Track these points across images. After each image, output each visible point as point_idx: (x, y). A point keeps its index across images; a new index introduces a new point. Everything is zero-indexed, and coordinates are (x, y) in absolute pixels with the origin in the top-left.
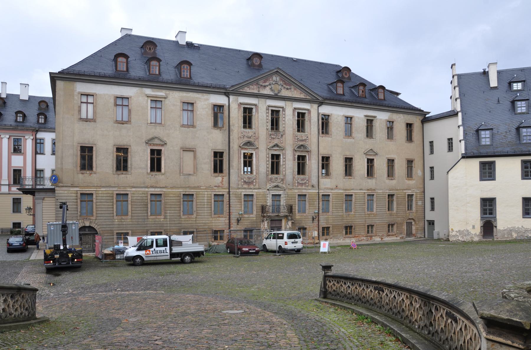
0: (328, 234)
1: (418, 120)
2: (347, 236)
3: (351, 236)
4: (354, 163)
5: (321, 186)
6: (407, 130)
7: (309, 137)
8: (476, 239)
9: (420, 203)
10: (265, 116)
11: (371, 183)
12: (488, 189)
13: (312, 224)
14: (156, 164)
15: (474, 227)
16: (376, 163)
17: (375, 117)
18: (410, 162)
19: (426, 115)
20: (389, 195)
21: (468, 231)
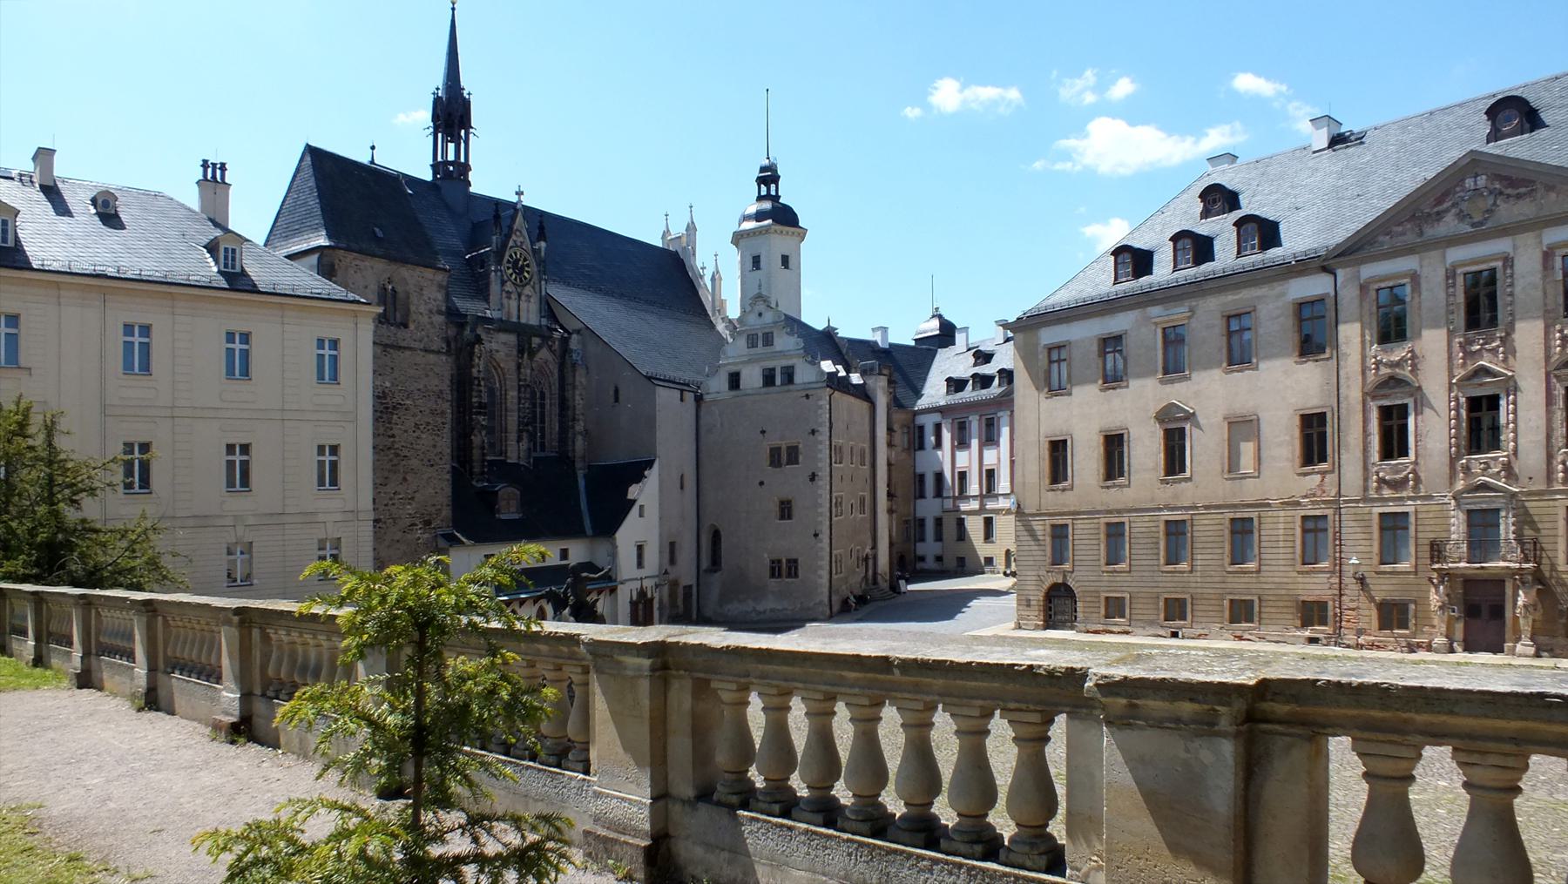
10: (1442, 295)
14: (1175, 460)
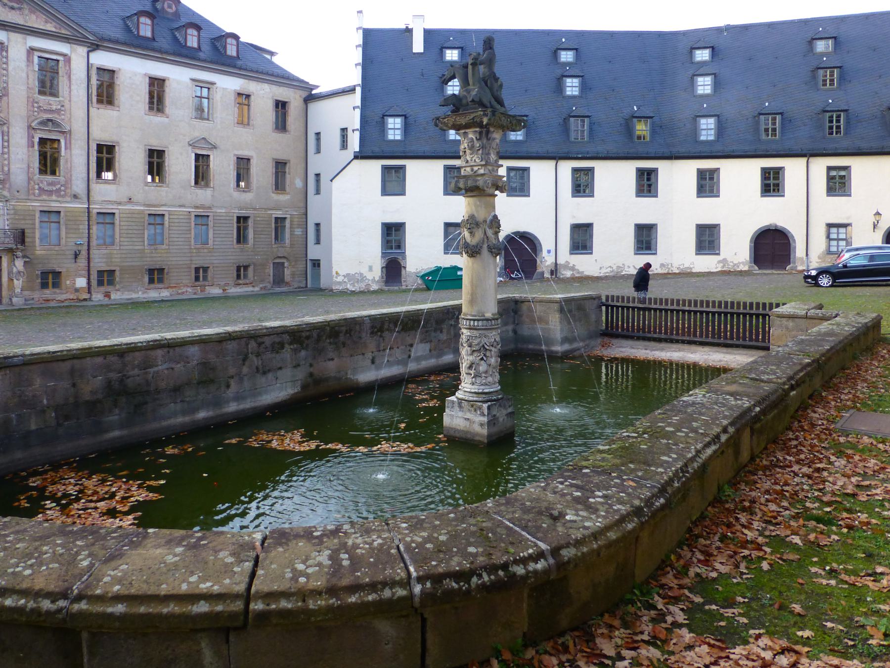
0: (111, 282)
1: (297, 97)
2: (152, 286)
3: (161, 286)
4: (167, 160)
5: (95, 196)
6: (277, 112)
7: (67, 106)
9: (298, 232)
11: (203, 196)
12: (394, 209)
13: (73, 265)
16: (213, 162)
17: (213, 84)
18: (280, 166)
19: (312, 89)
20: (239, 218)
21: (361, 274)
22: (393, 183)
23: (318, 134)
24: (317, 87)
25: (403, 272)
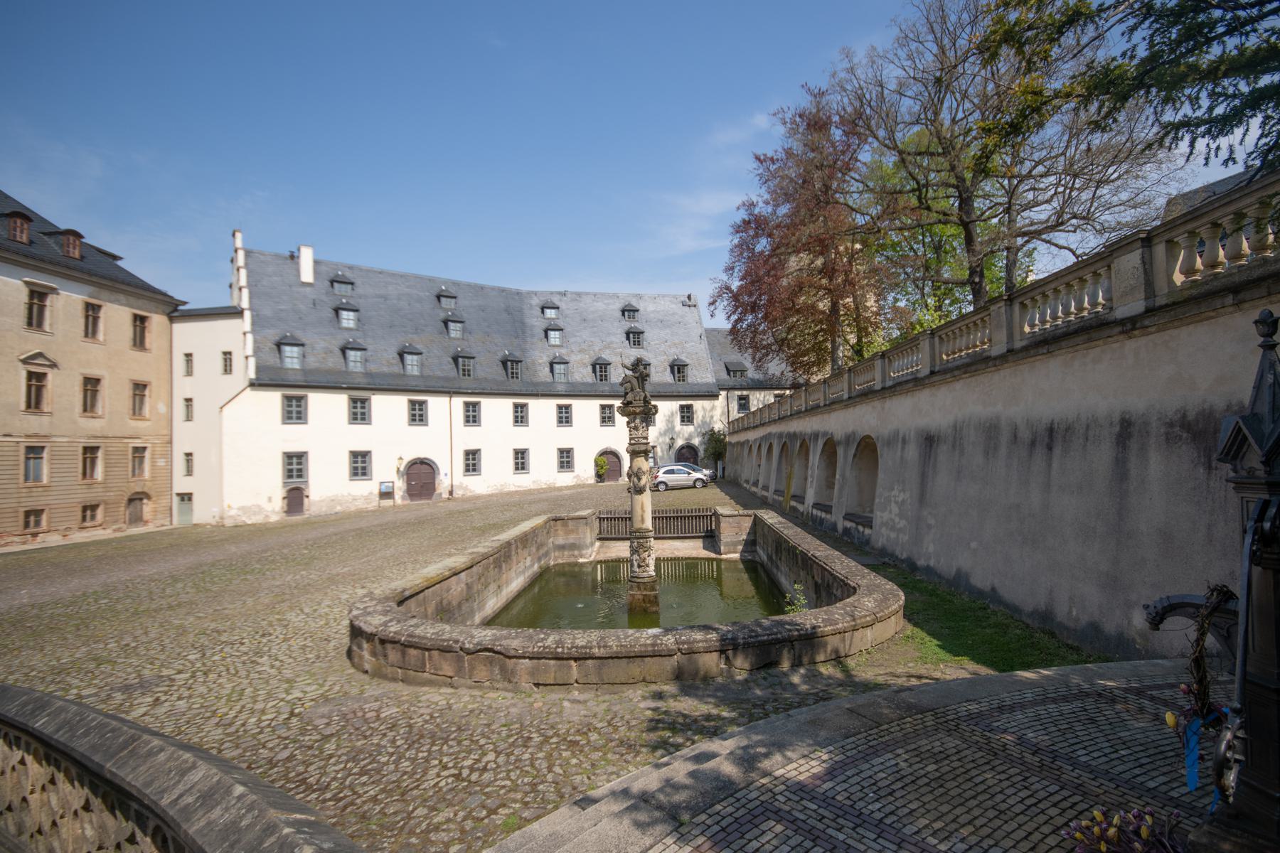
6: (135, 326)
8: (274, 518)
12: (294, 438)
15: (270, 499)
18: (140, 388)
20: (86, 449)
22: (295, 412)
23: (189, 356)
24: (185, 303)
25: (306, 500)
